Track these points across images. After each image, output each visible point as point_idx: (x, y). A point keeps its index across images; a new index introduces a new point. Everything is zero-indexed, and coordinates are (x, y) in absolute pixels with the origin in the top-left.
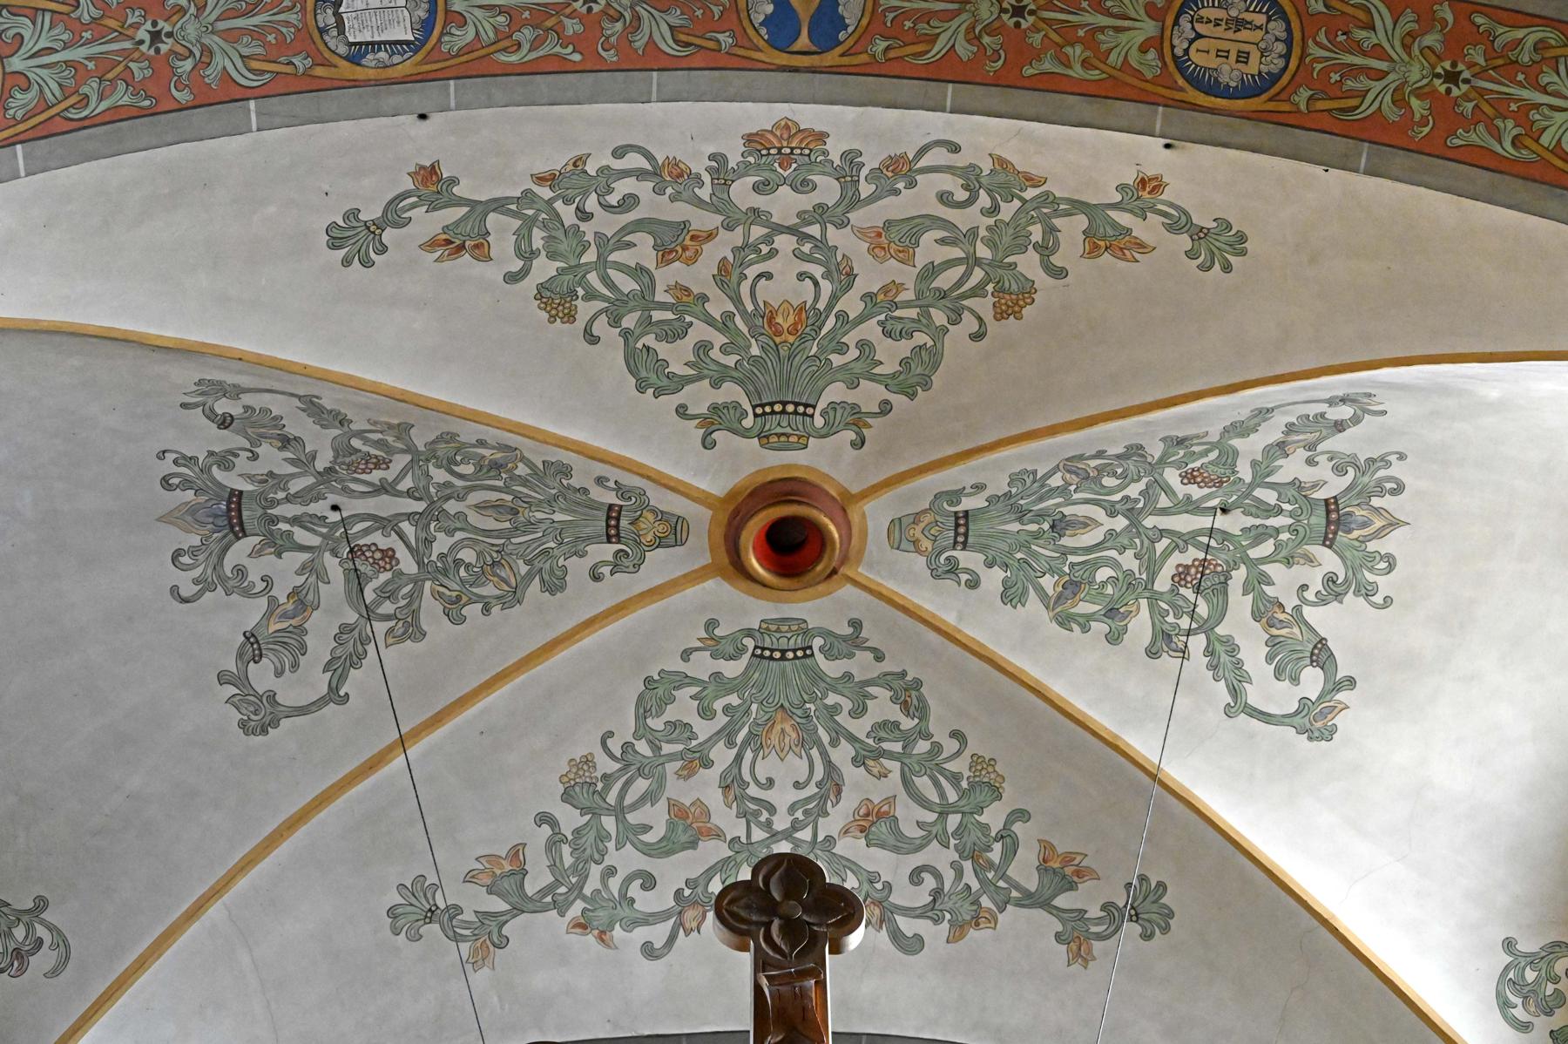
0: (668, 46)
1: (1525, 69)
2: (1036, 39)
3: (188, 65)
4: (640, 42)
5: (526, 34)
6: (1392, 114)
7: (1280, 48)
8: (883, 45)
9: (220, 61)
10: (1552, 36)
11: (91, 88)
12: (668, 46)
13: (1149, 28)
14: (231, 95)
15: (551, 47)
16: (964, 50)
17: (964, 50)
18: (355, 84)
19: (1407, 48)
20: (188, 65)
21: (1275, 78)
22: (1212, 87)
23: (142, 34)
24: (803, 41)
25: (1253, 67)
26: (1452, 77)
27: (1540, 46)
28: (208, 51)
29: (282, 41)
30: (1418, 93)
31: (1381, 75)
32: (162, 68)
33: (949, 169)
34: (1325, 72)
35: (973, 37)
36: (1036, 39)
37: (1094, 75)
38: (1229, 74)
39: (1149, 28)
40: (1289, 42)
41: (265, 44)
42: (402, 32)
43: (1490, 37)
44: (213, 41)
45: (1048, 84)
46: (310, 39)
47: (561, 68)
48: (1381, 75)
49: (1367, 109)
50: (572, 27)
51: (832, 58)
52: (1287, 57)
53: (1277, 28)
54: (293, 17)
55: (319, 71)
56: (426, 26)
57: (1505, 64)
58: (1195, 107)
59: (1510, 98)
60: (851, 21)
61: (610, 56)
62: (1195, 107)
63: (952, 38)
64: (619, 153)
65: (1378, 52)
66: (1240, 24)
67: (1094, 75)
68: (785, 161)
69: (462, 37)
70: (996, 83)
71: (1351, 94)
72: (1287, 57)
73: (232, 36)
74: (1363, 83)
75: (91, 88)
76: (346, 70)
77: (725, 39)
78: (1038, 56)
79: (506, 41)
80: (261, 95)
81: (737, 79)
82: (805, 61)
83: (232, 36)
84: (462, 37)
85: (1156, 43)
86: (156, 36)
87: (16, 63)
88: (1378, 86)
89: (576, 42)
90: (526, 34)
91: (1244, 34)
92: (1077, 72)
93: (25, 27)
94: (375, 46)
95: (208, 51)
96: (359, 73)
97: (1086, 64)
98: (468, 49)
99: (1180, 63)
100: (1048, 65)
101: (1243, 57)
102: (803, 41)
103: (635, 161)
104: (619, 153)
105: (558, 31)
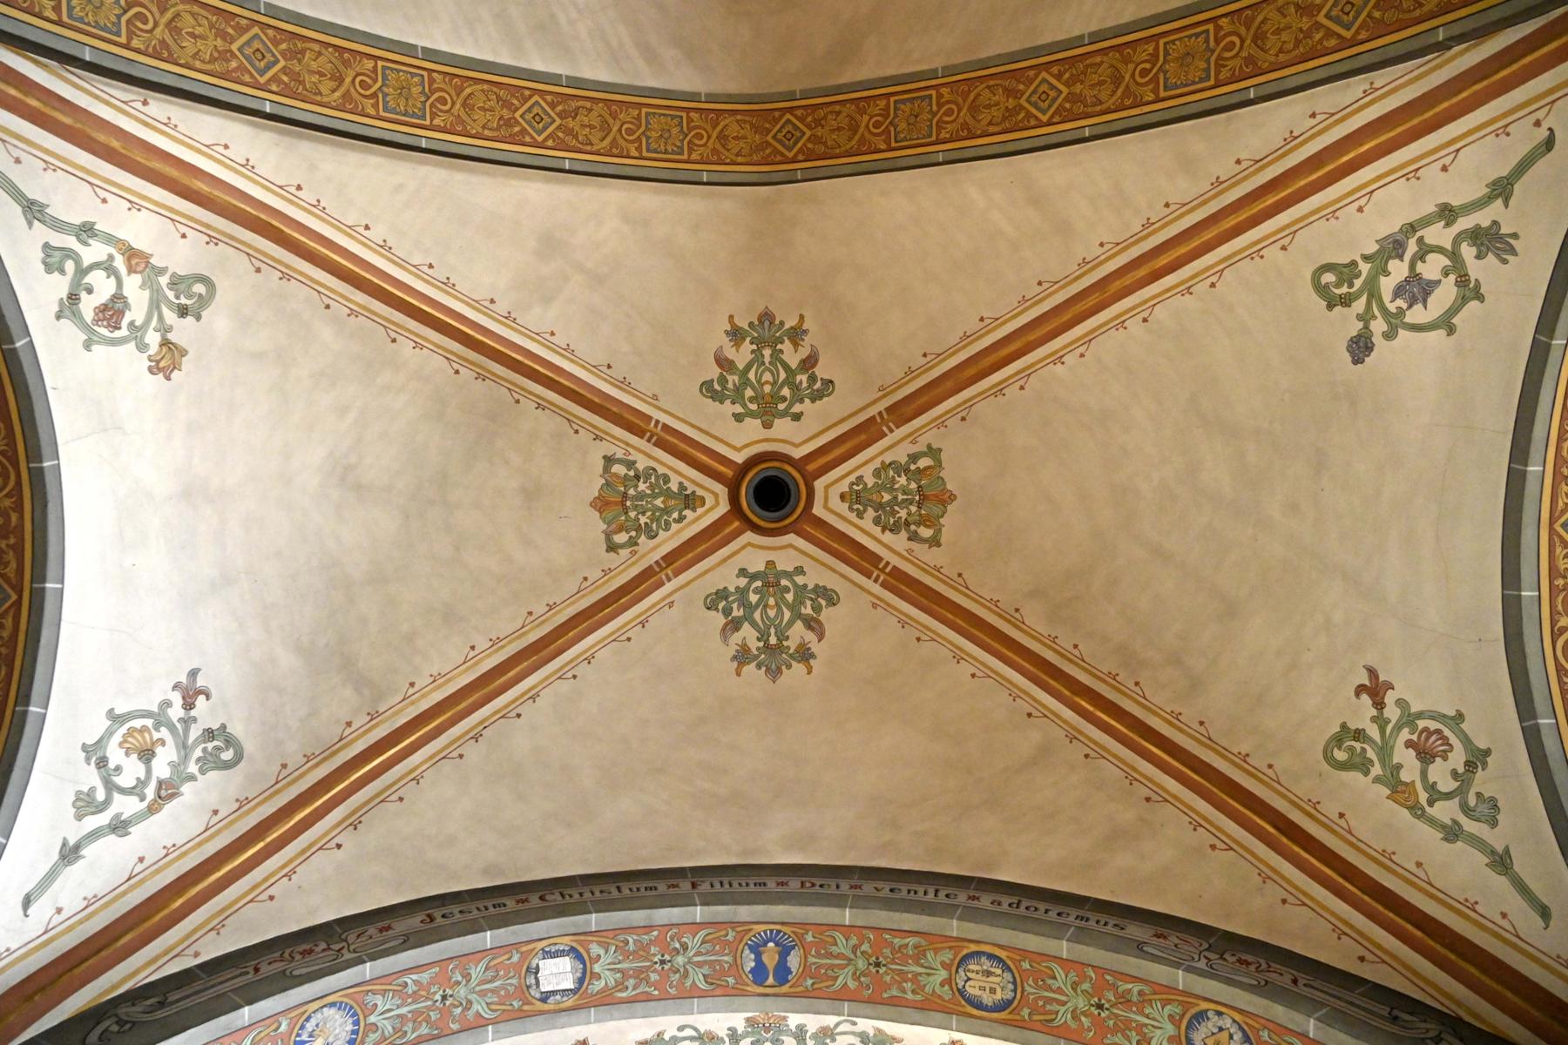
0: (702, 985)
1: (1135, 1004)
2: (888, 978)
3: (459, 1010)
4: (688, 983)
5: (631, 982)
6: (1073, 1025)
7: (1011, 986)
8: (810, 982)
9: (476, 1007)
10: (1147, 989)
11: (408, 1027)
12: (702, 985)
13: (943, 974)
14: (480, 1024)
15: (643, 988)
16: (852, 984)
17: (852, 984)
18: (542, 1013)
19: (1074, 990)
20: (459, 1010)
21: (1010, 1002)
22: (979, 1005)
23: (438, 997)
24: (771, 980)
25: (999, 996)
26: (1100, 1007)
27: (1141, 993)
28: (470, 1002)
29: (508, 994)
30: (1084, 1014)
31: (1064, 1004)
32: (446, 1013)
33: (853, 1033)
34: (1036, 1000)
35: (856, 977)
36: (888, 978)
37: (919, 997)
38: (987, 999)
39: (943, 974)
40: (1014, 983)
41: (499, 996)
42: (569, 984)
43: (1114, 987)
44: (473, 997)
45: (894, 1002)
46: (523, 991)
47: (648, 998)
48: (1064, 1004)
49: (1059, 1021)
50: (654, 977)
51: (785, 989)
52: (1015, 991)
53: (1008, 976)
54: (514, 981)
55: (526, 1008)
56: (581, 981)
57: (1124, 1000)
58: (972, 1016)
59: (1132, 1020)
60: (794, 970)
61: (673, 991)
62: (972, 1016)
63: (845, 978)
64: (681, 1029)
65: (1059, 991)
66: (988, 974)
67: (919, 997)
68: (767, 1030)
69: (598, 985)
70: (869, 1001)
71: (1050, 1013)
72: (1015, 991)
73: (483, 994)
74: (1055, 1007)
75: (408, 1027)
76: (539, 1006)
77: (731, 980)
78: (888, 987)
79: (620, 985)
80: (494, 1022)
81: (738, 1001)
82: (776, 990)
83: (483, 994)
84: (598, 985)
85: (948, 982)
86: (444, 998)
87: (372, 1019)
88: (1063, 1009)
89: (655, 985)
90: (631, 982)
91: (991, 979)
92: (910, 996)
93: (379, 1000)
94: (554, 993)
95: (470, 1002)
96: (546, 1007)
97: (913, 992)
98: (602, 991)
99: (961, 992)
100: (895, 992)
101: (993, 991)
102: (771, 980)
103: (689, 1032)
104: (681, 1029)
105: (647, 980)
